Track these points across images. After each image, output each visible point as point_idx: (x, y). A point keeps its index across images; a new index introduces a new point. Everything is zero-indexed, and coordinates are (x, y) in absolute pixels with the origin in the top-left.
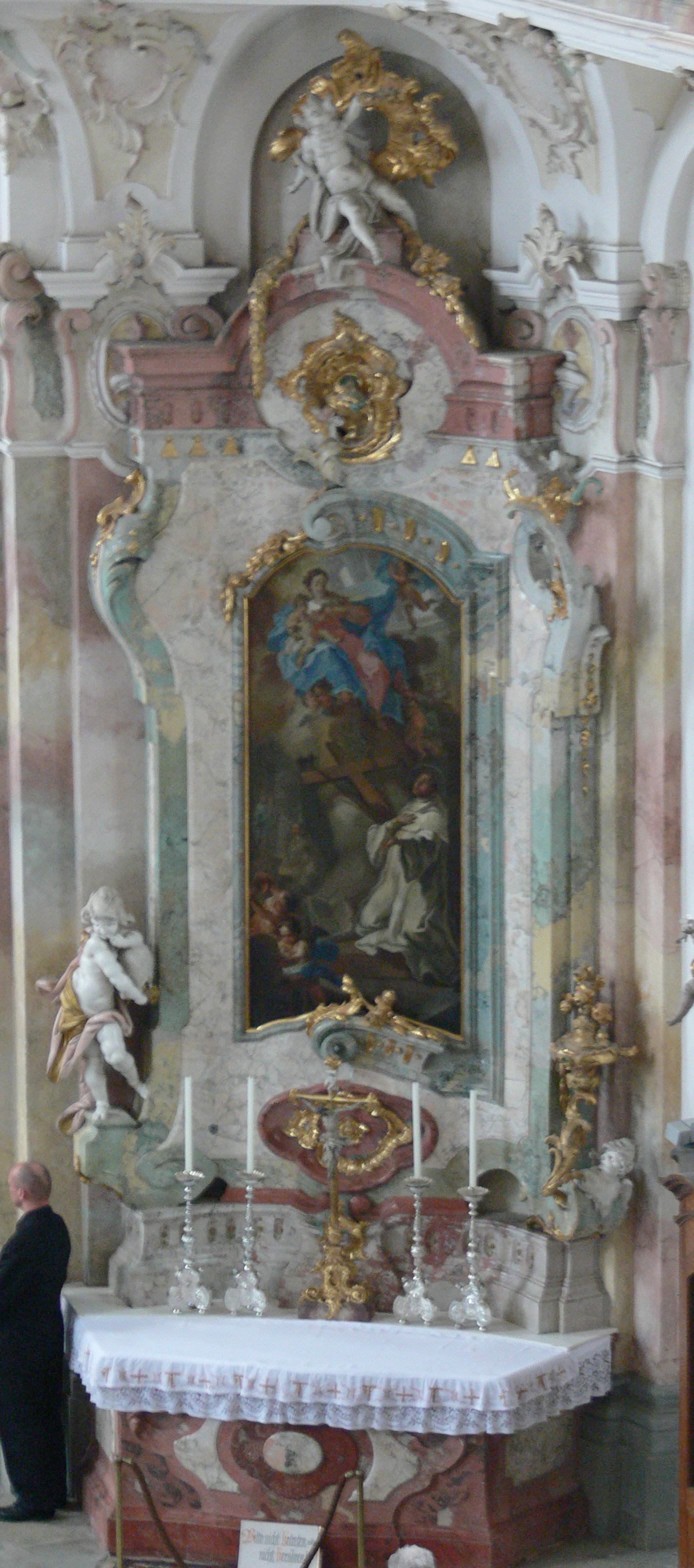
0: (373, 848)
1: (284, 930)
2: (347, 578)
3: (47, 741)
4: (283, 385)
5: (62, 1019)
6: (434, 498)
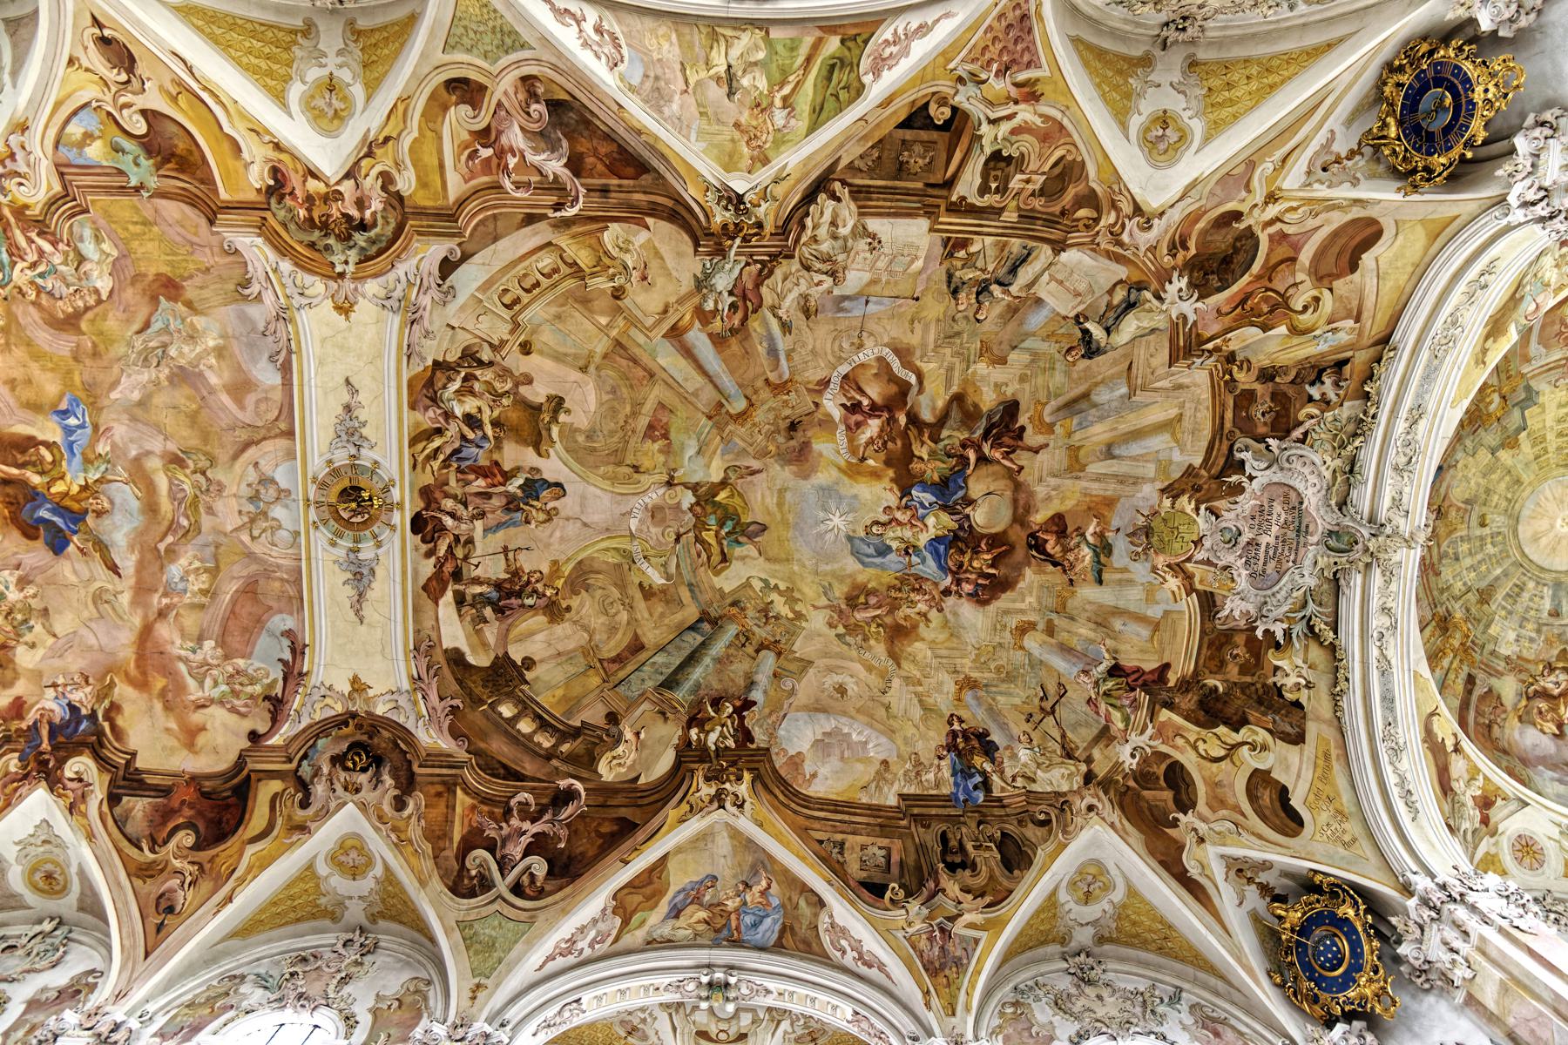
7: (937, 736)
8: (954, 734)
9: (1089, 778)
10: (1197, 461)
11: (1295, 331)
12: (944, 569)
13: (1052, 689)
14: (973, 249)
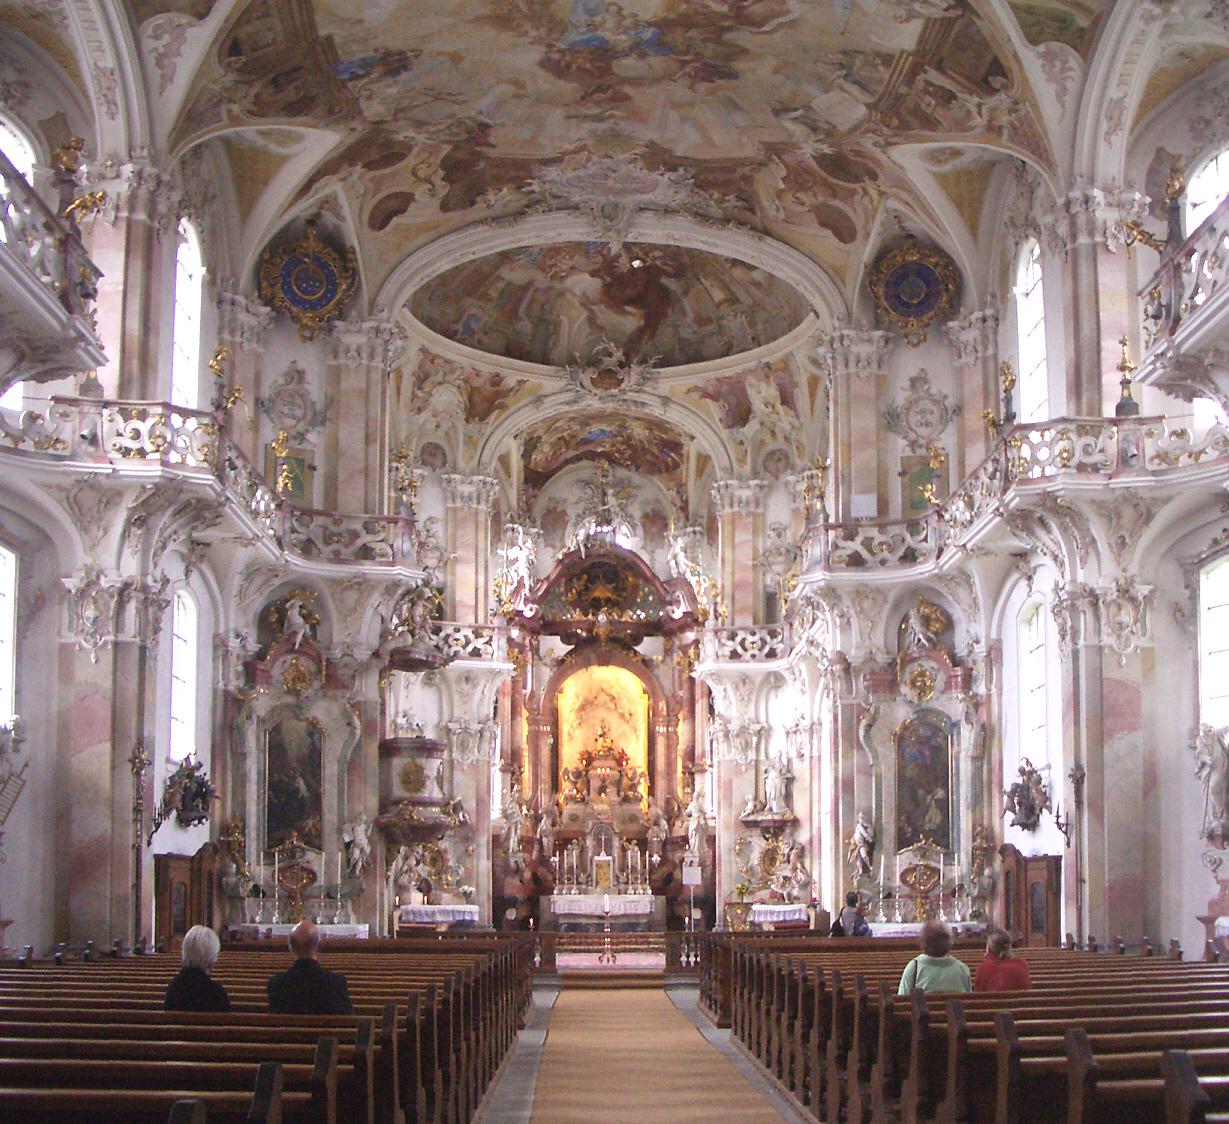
2: (921, 730)
5: (852, 847)
7: (394, 44)
8: (401, 53)
9: (382, 122)
10: (679, 154)
11: (779, 194)
12: (575, 44)
13: (461, 98)
14: (881, 68)
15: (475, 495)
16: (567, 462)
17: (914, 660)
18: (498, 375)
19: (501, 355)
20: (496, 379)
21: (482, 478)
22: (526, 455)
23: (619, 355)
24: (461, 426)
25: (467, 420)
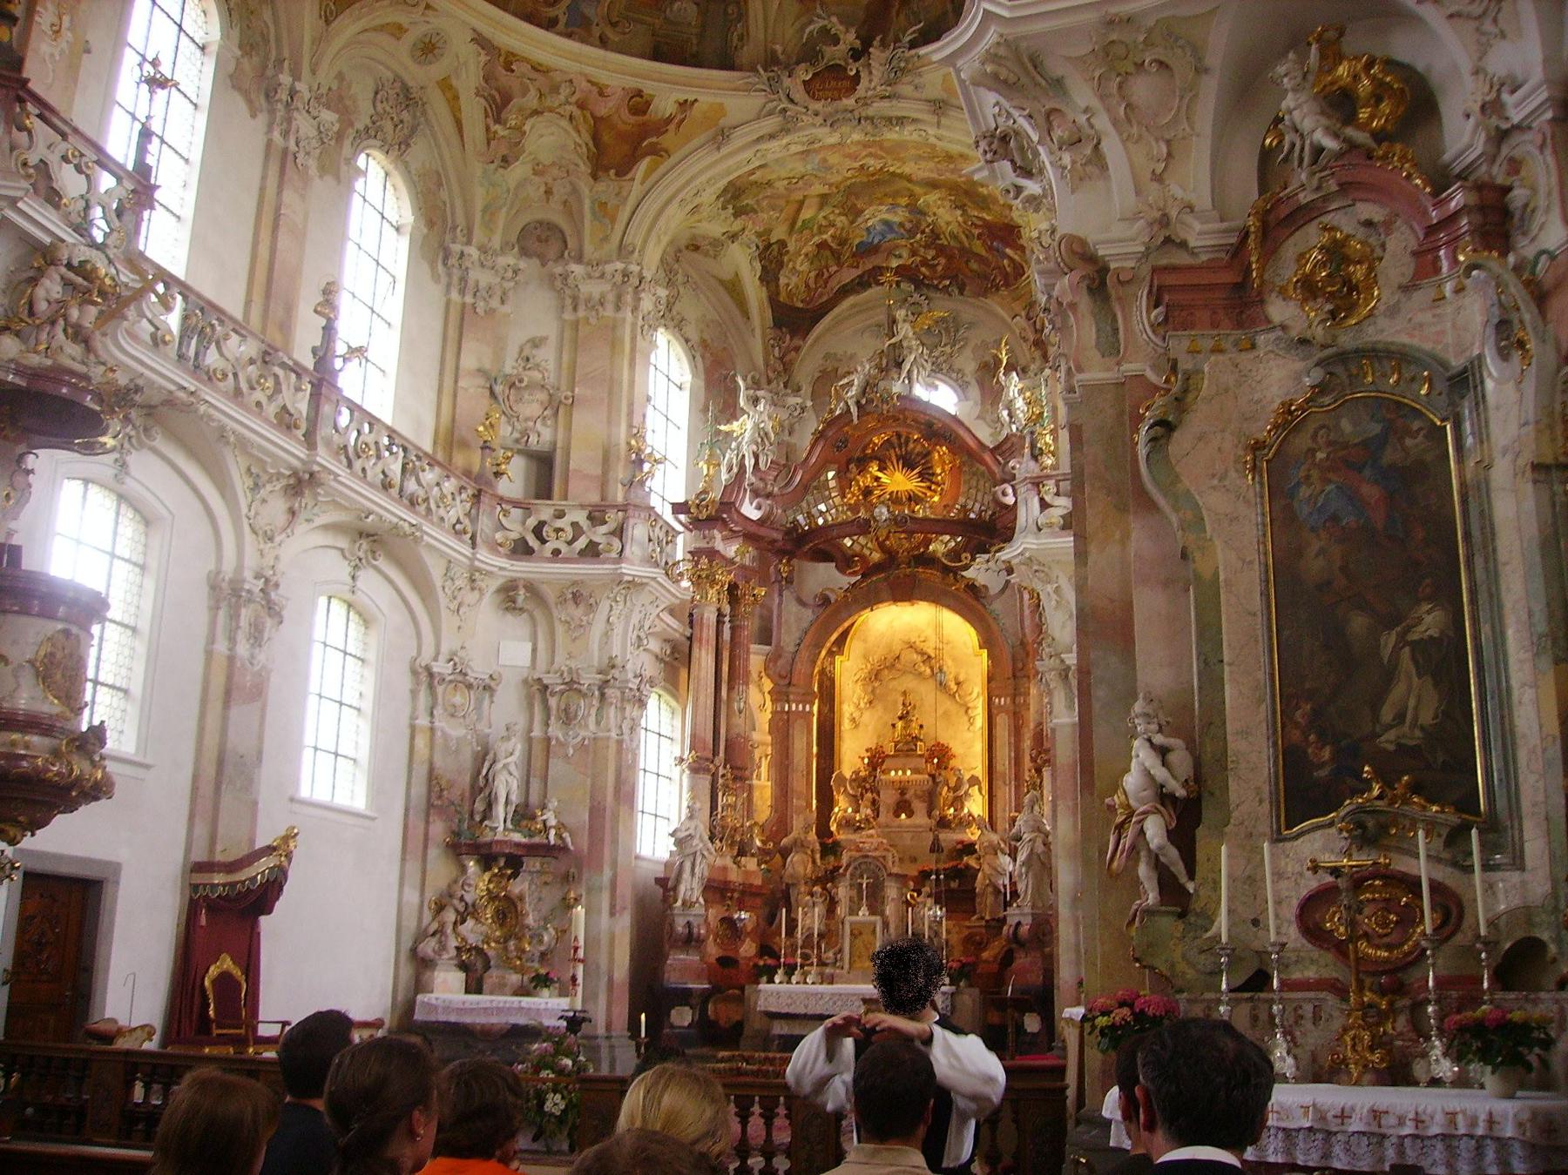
0: (1386, 653)
1: (1312, 737)
2: (1346, 425)
3: (1112, 601)
4: (1283, 292)
6: (1411, 336)
15: (611, 297)
16: (845, 292)
17: (1301, 216)
18: (639, 93)
19: (642, 56)
20: (639, 102)
21: (619, 266)
22: (769, 278)
23: (850, 38)
24: (585, 185)
25: (595, 177)
